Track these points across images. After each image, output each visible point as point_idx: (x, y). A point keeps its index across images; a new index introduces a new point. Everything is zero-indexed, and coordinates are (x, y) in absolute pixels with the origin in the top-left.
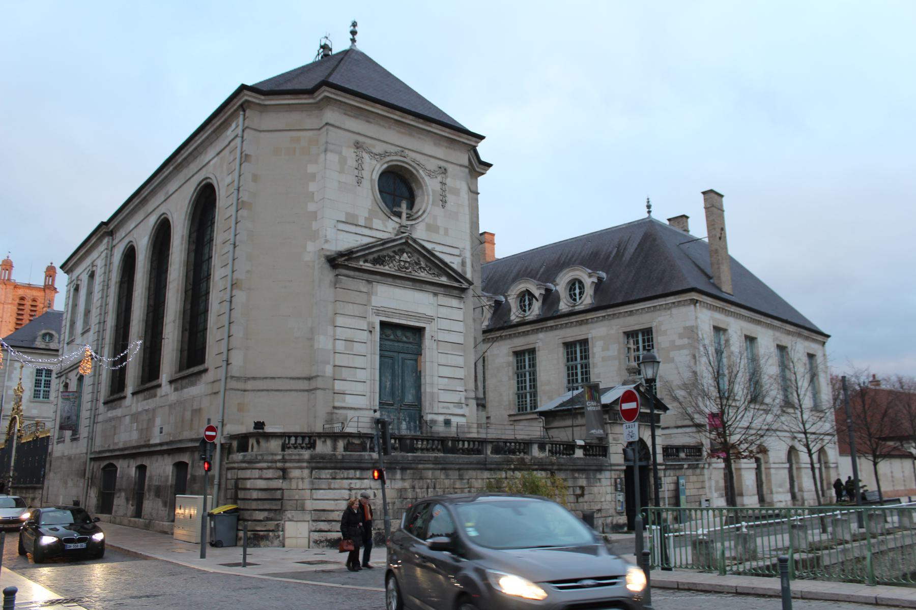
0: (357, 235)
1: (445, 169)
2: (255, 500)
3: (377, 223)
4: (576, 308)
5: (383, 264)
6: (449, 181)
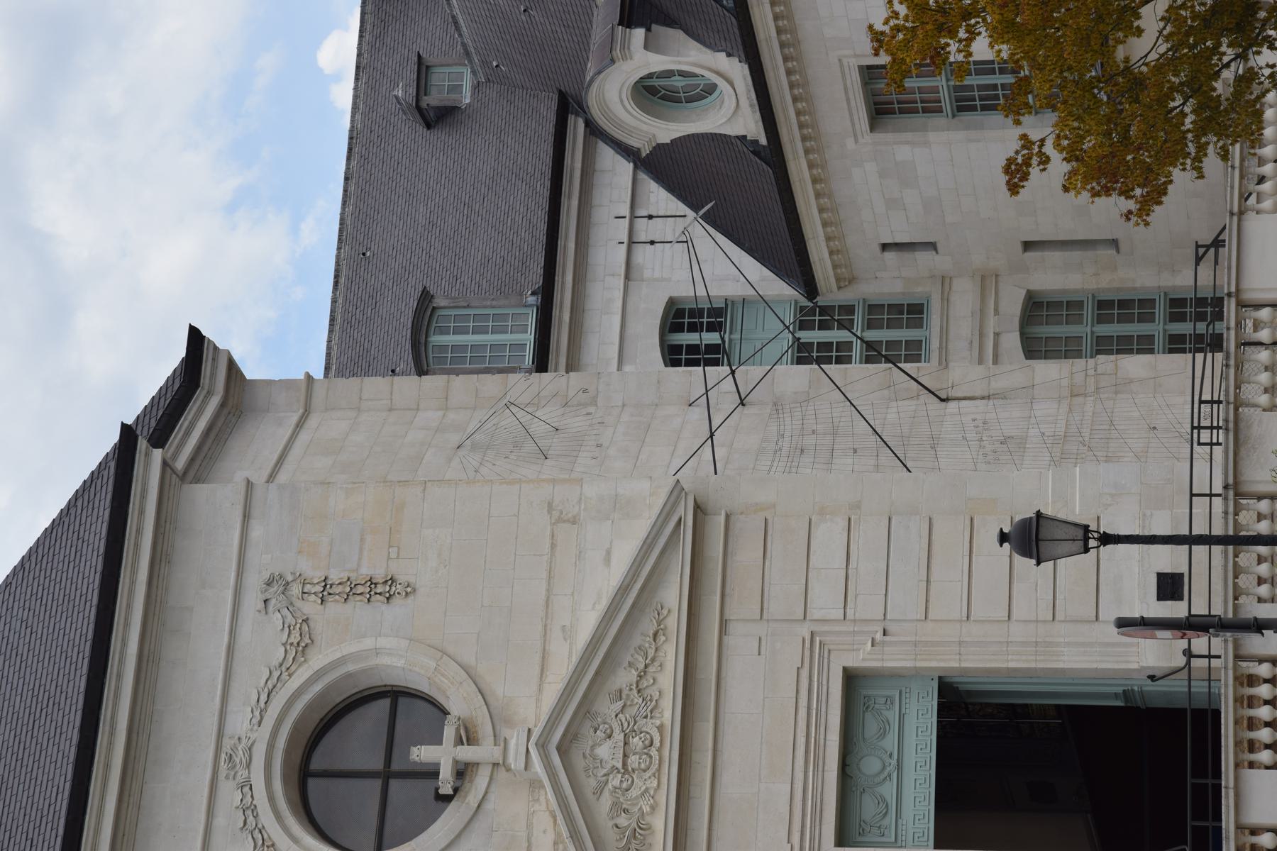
1: (269, 583)
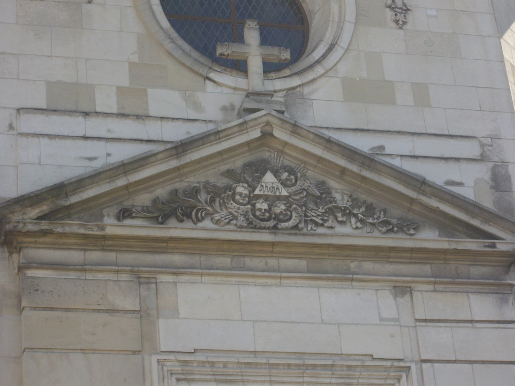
0: (89, 143)
5: (189, 216)
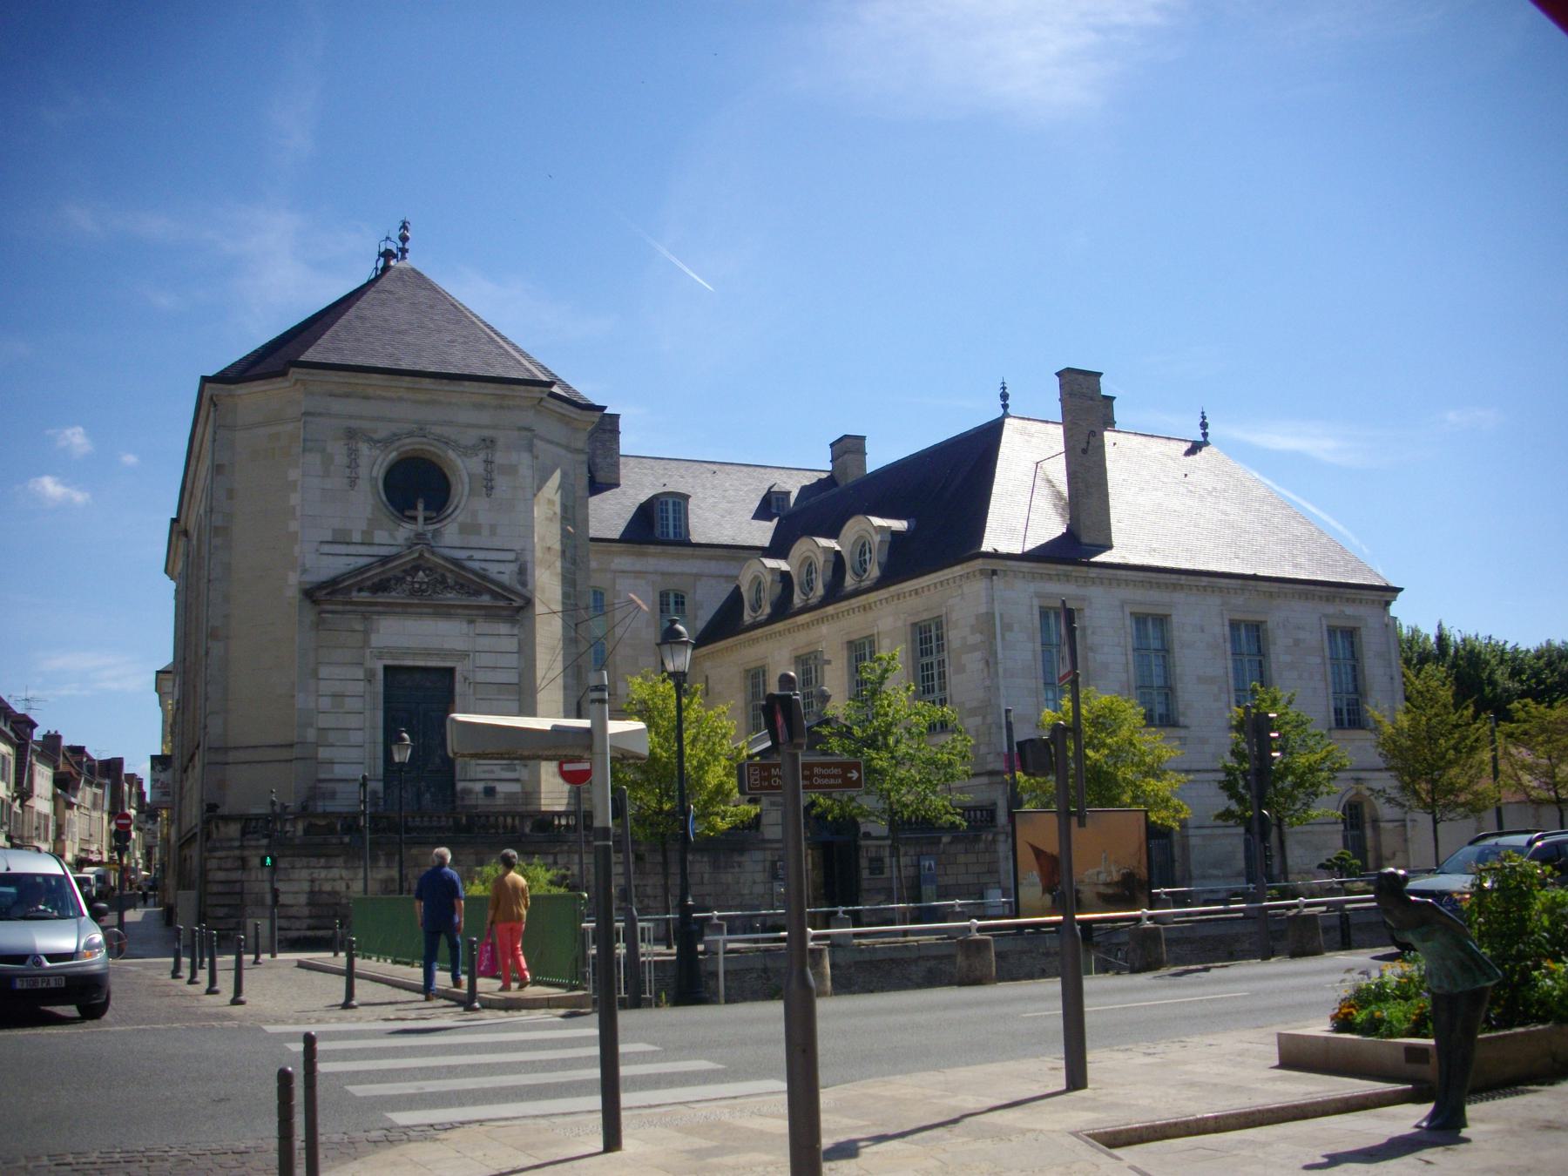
2: (215, 894)
3: (380, 536)
4: (862, 584)
6: (500, 458)
